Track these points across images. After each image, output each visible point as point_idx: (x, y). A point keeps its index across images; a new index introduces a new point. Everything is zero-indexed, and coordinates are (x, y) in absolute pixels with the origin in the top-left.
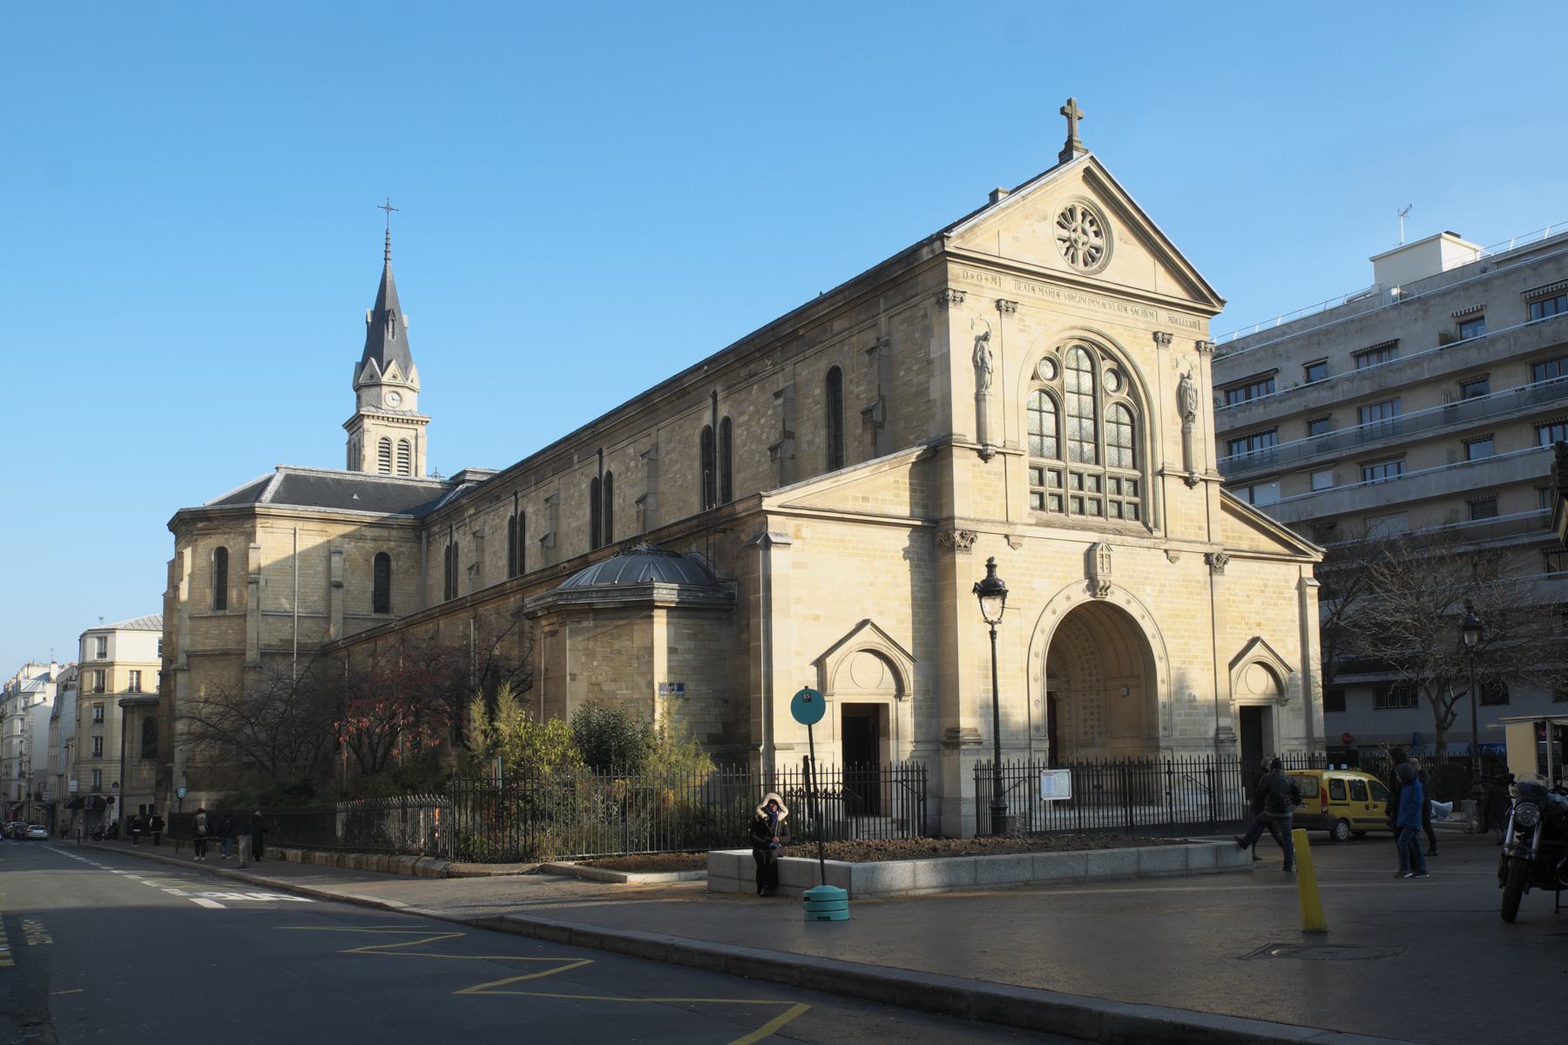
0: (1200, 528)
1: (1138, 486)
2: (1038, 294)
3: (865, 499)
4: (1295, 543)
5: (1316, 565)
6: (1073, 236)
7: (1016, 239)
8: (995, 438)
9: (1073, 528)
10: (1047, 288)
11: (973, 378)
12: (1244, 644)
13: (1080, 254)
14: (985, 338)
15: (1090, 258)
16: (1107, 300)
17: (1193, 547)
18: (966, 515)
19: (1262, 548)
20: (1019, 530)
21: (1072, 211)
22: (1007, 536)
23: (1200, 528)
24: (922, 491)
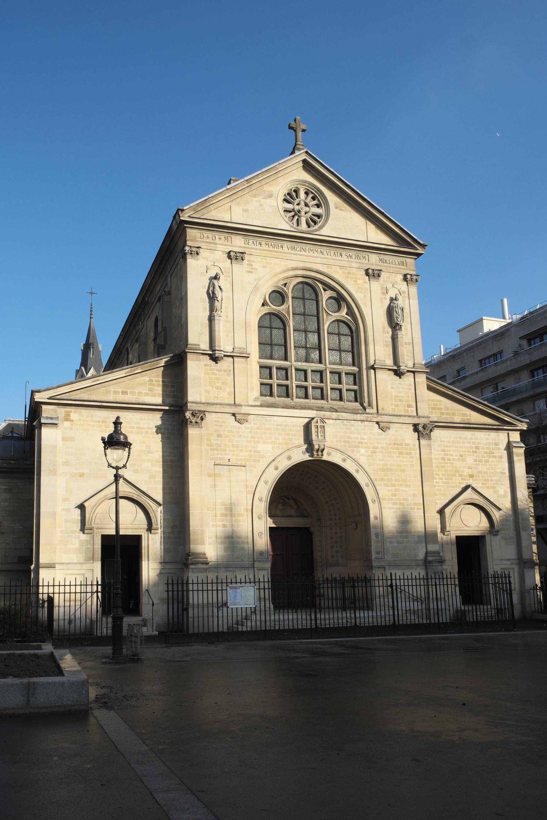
0: (409, 406)
1: (356, 378)
2: (264, 247)
3: (124, 393)
4: (502, 416)
5: (523, 434)
6: (297, 208)
7: (245, 211)
8: (224, 344)
9: (294, 408)
10: (273, 242)
11: (207, 305)
12: (459, 490)
13: (303, 220)
14: (216, 277)
15: (314, 220)
16: (324, 249)
17: (402, 420)
19: (473, 421)
20: (244, 410)
21: (296, 191)
22: (234, 415)
23: (409, 406)
24: (172, 386)
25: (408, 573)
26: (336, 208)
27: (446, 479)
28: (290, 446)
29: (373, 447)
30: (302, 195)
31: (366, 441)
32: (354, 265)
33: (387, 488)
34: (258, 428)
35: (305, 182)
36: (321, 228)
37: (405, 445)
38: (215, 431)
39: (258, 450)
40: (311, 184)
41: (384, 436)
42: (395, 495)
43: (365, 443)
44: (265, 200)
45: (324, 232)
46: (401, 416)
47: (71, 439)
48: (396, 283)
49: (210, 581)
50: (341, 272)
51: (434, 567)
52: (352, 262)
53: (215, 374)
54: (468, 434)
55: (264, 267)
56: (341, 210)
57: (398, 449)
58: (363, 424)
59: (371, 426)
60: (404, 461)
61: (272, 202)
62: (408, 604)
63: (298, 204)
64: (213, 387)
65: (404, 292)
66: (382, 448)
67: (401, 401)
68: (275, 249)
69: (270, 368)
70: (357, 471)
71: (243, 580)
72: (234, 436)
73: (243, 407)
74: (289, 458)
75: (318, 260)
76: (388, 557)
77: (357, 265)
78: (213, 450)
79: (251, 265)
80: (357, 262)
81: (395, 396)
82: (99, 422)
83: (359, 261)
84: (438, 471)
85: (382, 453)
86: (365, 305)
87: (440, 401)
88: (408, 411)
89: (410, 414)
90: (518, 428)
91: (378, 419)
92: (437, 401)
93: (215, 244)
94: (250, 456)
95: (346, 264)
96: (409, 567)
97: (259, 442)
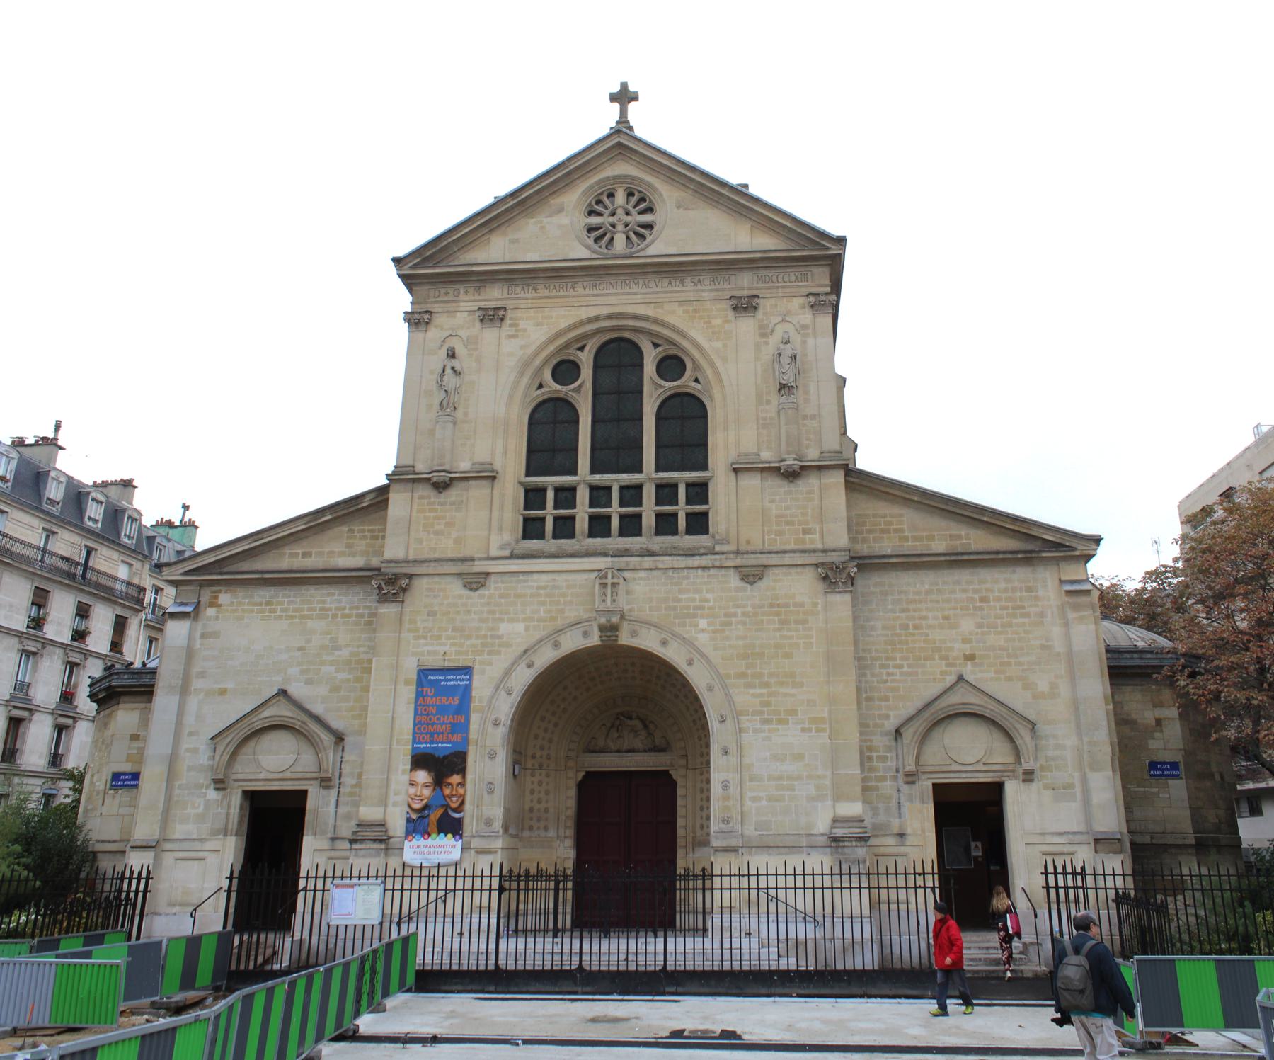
2: (542, 292)
3: (305, 555)
6: (611, 219)
17: (787, 560)
18: (401, 554)
20: (479, 567)
21: (611, 195)
23: (806, 532)
25: (795, 862)
28: (559, 623)
29: (726, 615)
30: (620, 198)
31: (711, 604)
32: (705, 295)
33: (752, 691)
34: (501, 596)
35: (626, 177)
36: (648, 246)
40: (634, 178)
43: (710, 608)
45: (651, 251)
46: (785, 552)
47: (215, 635)
48: (789, 313)
50: (680, 310)
51: (846, 850)
53: (436, 510)
54: (964, 575)
55: (538, 325)
57: (778, 614)
60: (791, 637)
61: (564, 220)
62: (782, 926)
63: (613, 214)
64: (429, 532)
65: (805, 327)
66: (744, 614)
67: (787, 523)
68: (562, 293)
69: (542, 491)
70: (690, 663)
71: (364, 873)
72: (458, 613)
74: (556, 645)
76: (750, 830)
77: (713, 295)
78: (418, 638)
79: (515, 325)
80: (711, 291)
81: (778, 517)
82: (261, 604)
83: (718, 287)
85: (744, 623)
86: (725, 360)
88: (803, 542)
89: (808, 546)
90: (1077, 553)
91: (739, 561)
94: (483, 645)
95: (691, 296)
96: (793, 849)
97: (502, 620)
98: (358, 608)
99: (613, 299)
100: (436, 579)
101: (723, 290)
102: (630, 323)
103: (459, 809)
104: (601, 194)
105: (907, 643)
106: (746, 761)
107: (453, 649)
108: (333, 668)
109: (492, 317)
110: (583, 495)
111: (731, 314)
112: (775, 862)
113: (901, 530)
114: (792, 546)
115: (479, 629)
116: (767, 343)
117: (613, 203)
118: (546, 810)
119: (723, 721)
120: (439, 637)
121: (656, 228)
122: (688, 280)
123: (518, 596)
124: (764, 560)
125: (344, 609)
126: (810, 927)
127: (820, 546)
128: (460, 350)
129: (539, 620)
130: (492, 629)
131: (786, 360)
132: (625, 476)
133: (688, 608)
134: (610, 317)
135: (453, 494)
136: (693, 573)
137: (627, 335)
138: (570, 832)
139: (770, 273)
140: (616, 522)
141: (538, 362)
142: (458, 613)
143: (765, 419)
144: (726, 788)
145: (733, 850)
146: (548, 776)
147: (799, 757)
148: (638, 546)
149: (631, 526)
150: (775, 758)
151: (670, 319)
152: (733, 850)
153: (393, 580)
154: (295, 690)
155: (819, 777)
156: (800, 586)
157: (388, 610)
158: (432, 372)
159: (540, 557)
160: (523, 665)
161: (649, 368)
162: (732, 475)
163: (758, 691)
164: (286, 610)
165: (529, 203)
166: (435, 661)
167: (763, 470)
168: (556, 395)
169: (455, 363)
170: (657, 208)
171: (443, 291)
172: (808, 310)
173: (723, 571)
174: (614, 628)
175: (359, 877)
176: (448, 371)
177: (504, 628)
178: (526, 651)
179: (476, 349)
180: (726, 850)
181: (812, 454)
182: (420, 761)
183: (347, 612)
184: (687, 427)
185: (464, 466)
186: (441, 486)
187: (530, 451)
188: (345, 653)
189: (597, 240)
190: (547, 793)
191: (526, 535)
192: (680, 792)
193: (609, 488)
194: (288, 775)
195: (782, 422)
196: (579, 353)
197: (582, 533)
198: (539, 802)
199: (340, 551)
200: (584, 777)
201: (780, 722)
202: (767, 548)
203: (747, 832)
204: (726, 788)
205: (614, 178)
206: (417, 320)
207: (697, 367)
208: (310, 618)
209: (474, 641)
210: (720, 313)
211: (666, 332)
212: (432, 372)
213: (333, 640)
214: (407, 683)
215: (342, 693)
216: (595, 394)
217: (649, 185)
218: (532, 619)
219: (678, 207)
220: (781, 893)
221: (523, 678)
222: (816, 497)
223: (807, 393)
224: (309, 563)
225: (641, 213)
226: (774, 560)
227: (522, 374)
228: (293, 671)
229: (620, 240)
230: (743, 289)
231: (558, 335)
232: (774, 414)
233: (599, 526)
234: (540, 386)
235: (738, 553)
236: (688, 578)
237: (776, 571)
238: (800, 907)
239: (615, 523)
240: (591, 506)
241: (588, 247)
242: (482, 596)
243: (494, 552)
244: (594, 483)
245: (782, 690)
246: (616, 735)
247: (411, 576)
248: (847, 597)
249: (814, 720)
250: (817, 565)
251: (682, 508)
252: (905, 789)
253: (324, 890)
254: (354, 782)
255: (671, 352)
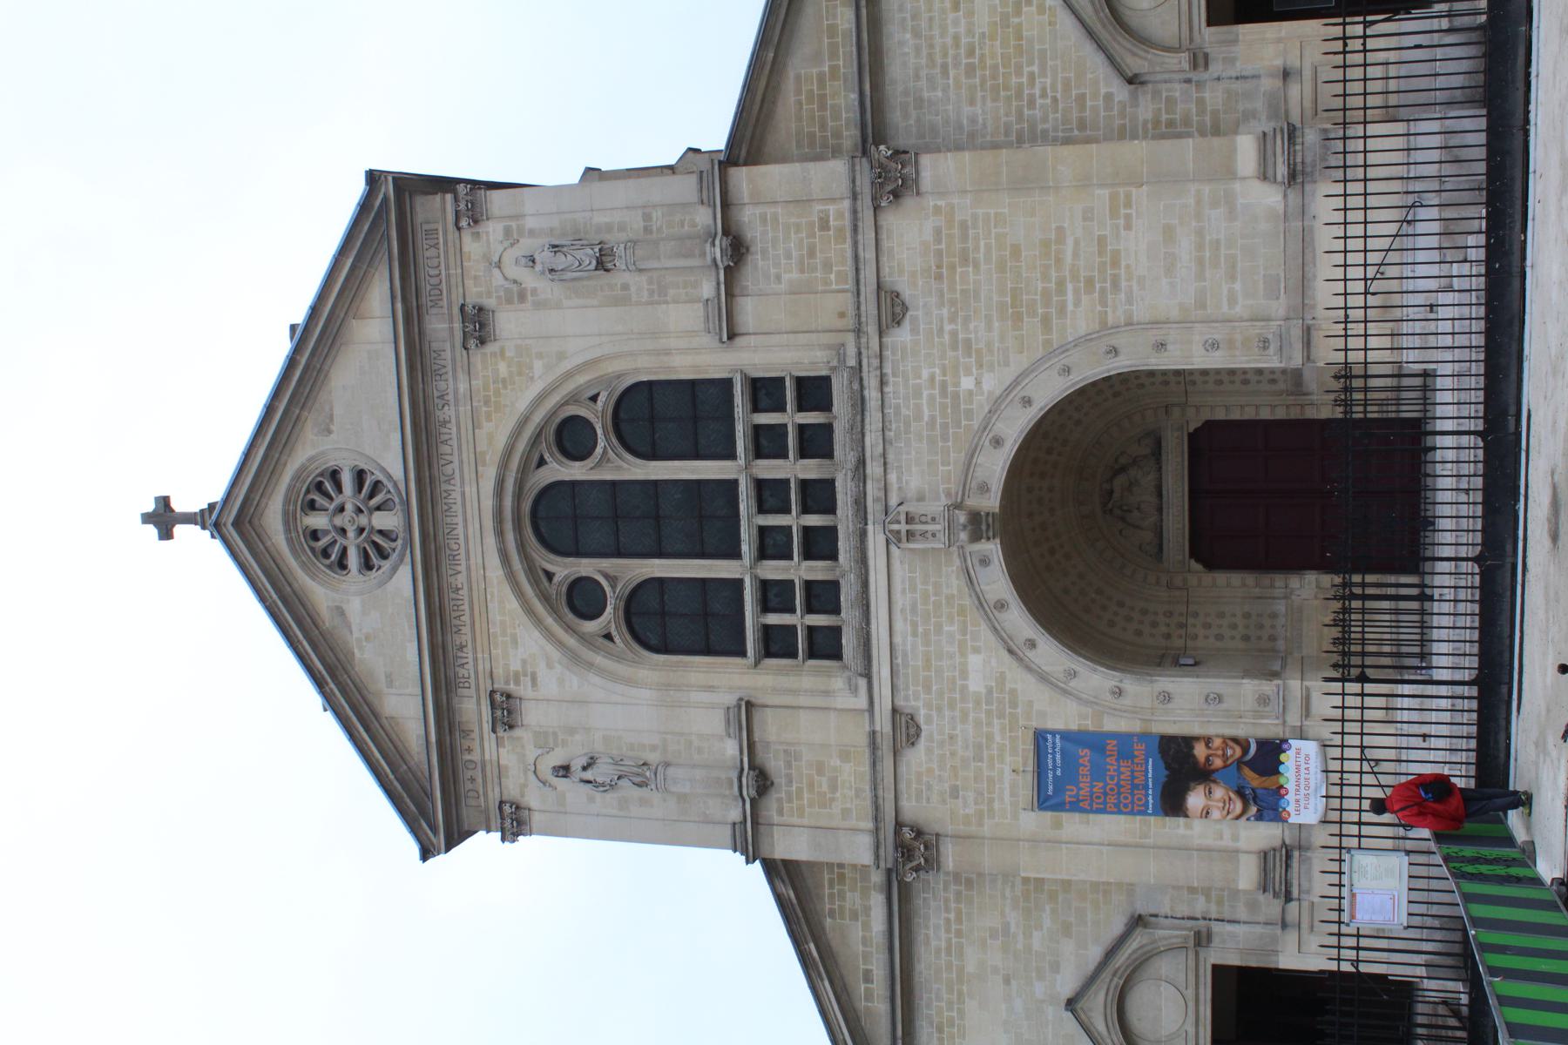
2: (466, 636)
3: (868, 977)
17: (868, 254)
20: (883, 724)
21: (315, 535)
23: (825, 226)
25: (1326, 238)
26: (330, 432)
27: (1030, 63)
28: (968, 602)
29: (954, 347)
30: (318, 521)
32: (463, 387)
33: (1070, 307)
34: (928, 689)
35: (286, 513)
36: (390, 477)
37: (940, 242)
38: (944, 802)
39: (984, 691)
40: (287, 501)
41: (920, 313)
42: (1090, 282)
44: (354, 628)
45: (397, 472)
48: (486, 257)
49: (1335, 841)
50: (487, 427)
51: (1308, 160)
52: (456, 391)
53: (800, 790)
55: (515, 642)
56: (331, 418)
57: (952, 268)
58: (891, 379)
59: (893, 354)
60: (988, 248)
61: (354, 606)
62: (1421, 256)
63: (343, 531)
64: (832, 800)
65: (508, 232)
66: (952, 320)
67: (812, 254)
68: (466, 607)
69: (767, 632)
70: (1027, 402)
72: (953, 754)
73: (878, 728)
74: (1001, 605)
75: (470, 490)
76: (1279, 307)
77: (462, 376)
78: (991, 810)
80: (455, 378)
81: (802, 271)
83: (449, 368)
84: (1006, 88)
85: (967, 320)
86: (561, 356)
87: (798, 77)
88: (840, 230)
89: (847, 222)
91: (872, 329)
92: (798, 92)
93: (483, 763)
94: (1001, 716)
95: (465, 409)
96: (1306, 239)
97: (964, 688)
98: (947, 900)
99: (474, 529)
100: (902, 786)
101: (454, 360)
102: (508, 502)
103: (1243, 744)
104: (313, 549)
105: (995, 67)
106: (1175, 314)
107: (1008, 759)
108: (1035, 933)
109: (505, 711)
110: (773, 570)
111: (491, 348)
112: (1326, 268)
113: (821, 79)
114: (848, 246)
115: (978, 723)
116: (534, 291)
117: (326, 532)
118: (1247, 616)
119: (1114, 351)
120: (991, 780)
121: (365, 467)
122: (440, 415)
123: (927, 667)
124: (869, 289)
125: (948, 920)
126: (1422, 213)
127: (847, 204)
128: (557, 758)
129: (964, 632)
130: (978, 703)
131: (561, 261)
132: (742, 507)
133: (944, 407)
134: (500, 533)
135: (774, 764)
136: (891, 400)
137: (527, 506)
138: (1279, 579)
139: (426, 288)
140: (813, 518)
141: (571, 641)
142: (953, 754)
143: (651, 292)
144: (1215, 345)
145: (1307, 332)
146: (1196, 615)
147: (1169, 233)
148: (850, 484)
149: (818, 496)
150: (1170, 270)
151: (501, 441)
152: (1307, 332)
153: (905, 850)
154: (1067, 985)
155: (1199, 202)
156: (909, 233)
157: (950, 856)
158: (591, 799)
159: (868, 634)
160: (1030, 654)
161: (576, 471)
162: (739, 341)
163: (1070, 297)
164: (950, 1003)
165: (331, 658)
166: (1026, 787)
167: (730, 295)
168: (621, 613)
169: (576, 766)
170: (331, 464)
171: (469, 786)
172: (481, 228)
173: (888, 353)
174: (975, 518)
175: (1341, 885)
176: (588, 775)
177: (976, 685)
178: (1010, 651)
179: (555, 734)
180: (1307, 343)
181: (704, 217)
182: (1172, 803)
183: (952, 916)
184: (664, 412)
185: (731, 749)
186: (763, 782)
187: (708, 651)
188: (1013, 918)
189: (384, 555)
190: (1221, 615)
191: (836, 655)
192: (1220, 415)
193: (762, 530)
194: (1190, 993)
195: (655, 265)
196: (556, 579)
197: (833, 569)
198: (1234, 626)
199: (863, 930)
200: (1198, 561)
201: (1115, 263)
202: (850, 285)
203: (1282, 312)
204: (1215, 345)
205: (288, 530)
206: (514, 823)
207: (573, 399)
208: (961, 969)
209: (996, 729)
210: (489, 365)
211: (521, 446)
212: (591, 799)
213: (993, 934)
214: (1058, 825)
215: (1072, 919)
216: (619, 554)
217: (297, 477)
218: (962, 644)
219: (330, 432)
220: (1373, 258)
221: (1050, 654)
222: (770, 210)
223: (609, 228)
224: (879, 970)
225: (339, 489)
226: (869, 274)
227: (590, 665)
228: (1039, 989)
229: (383, 520)
230: (451, 330)
231: (529, 611)
232: (643, 278)
233: (820, 544)
234: (608, 637)
235: (858, 331)
236: (898, 407)
237: (885, 271)
238: (1392, 229)
239: (814, 520)
240: (790, 558)
241: (394, 569)
242: (929, 719)
243: (862, 702)
244: (754, 553)
245: (1069, 259)
246: (1136, 513)
247: (899, 825)
248: (926, 160)
249: (1114, 213)
250: (876, 208)
251: (791, 418)
252: (1216, 68)
253: (1358, 936)
254: (1202, 899)
255: (552, 438)
